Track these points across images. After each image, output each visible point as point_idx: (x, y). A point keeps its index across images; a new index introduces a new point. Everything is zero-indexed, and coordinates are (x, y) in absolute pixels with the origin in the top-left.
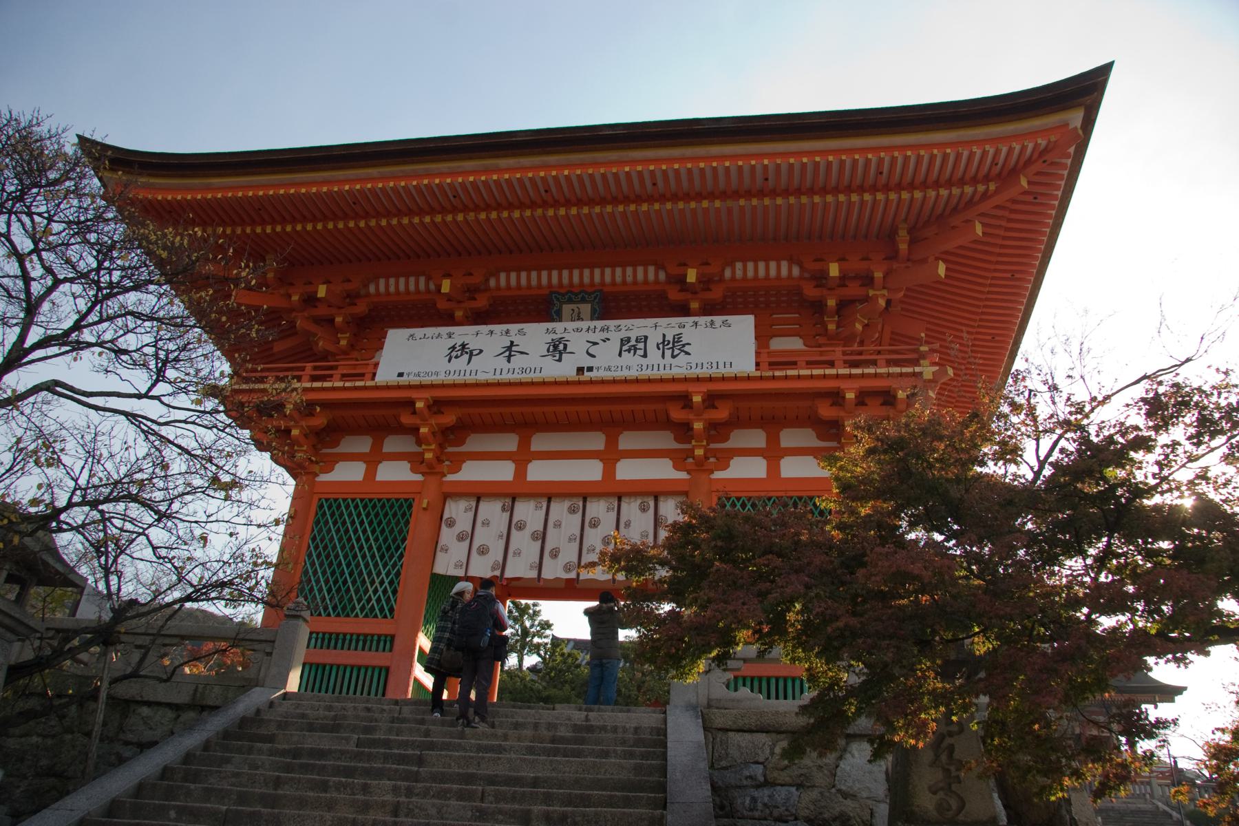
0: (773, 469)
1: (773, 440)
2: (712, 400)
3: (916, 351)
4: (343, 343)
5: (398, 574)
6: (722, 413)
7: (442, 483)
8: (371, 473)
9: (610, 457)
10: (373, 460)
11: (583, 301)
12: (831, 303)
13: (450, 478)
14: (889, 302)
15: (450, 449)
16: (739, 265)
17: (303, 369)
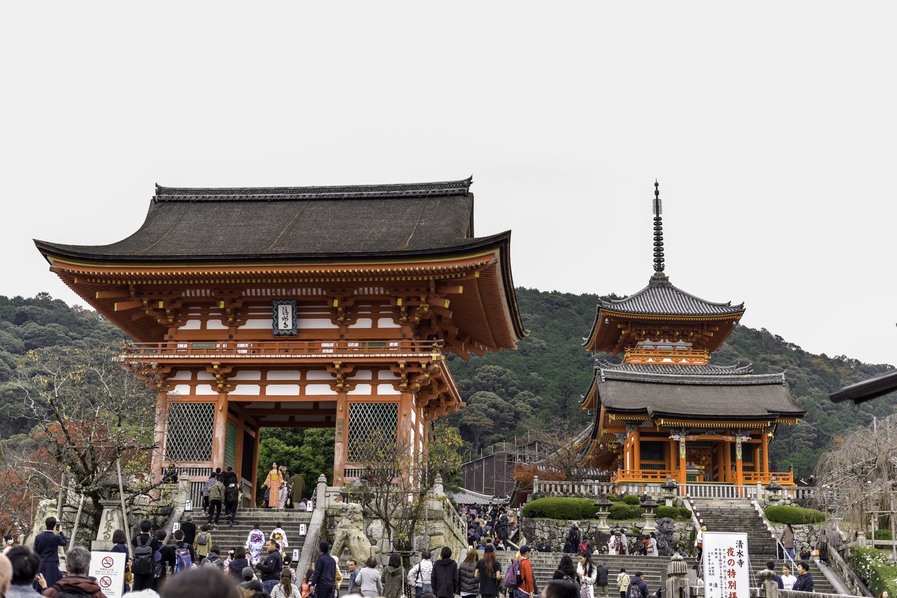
0: (374, 390)
1: (375, 376)
2: (344, 365)
3: (431, 344)
4: (170, 320)
5: (211, 440)
6: (349, 370)
7: (227, 396)
8: (193, 391)
9: (303, 383)
10: (193, 383)
11: (288, 304)
12: (403, 309)
13: (231, 393)
14: (430, 308)
15: (229, 379)
16: (361, 289)
17: (157, 346)
